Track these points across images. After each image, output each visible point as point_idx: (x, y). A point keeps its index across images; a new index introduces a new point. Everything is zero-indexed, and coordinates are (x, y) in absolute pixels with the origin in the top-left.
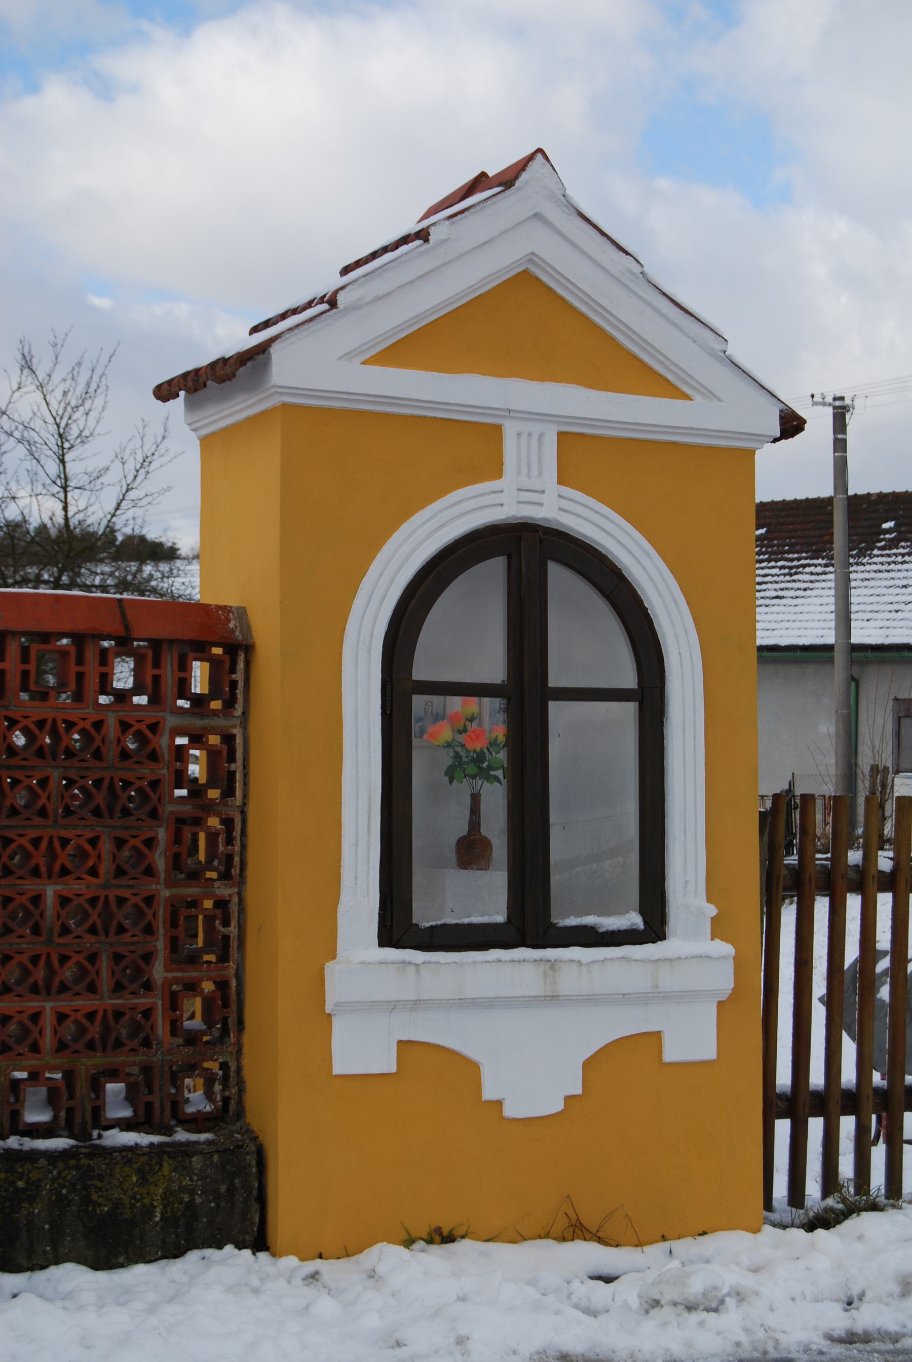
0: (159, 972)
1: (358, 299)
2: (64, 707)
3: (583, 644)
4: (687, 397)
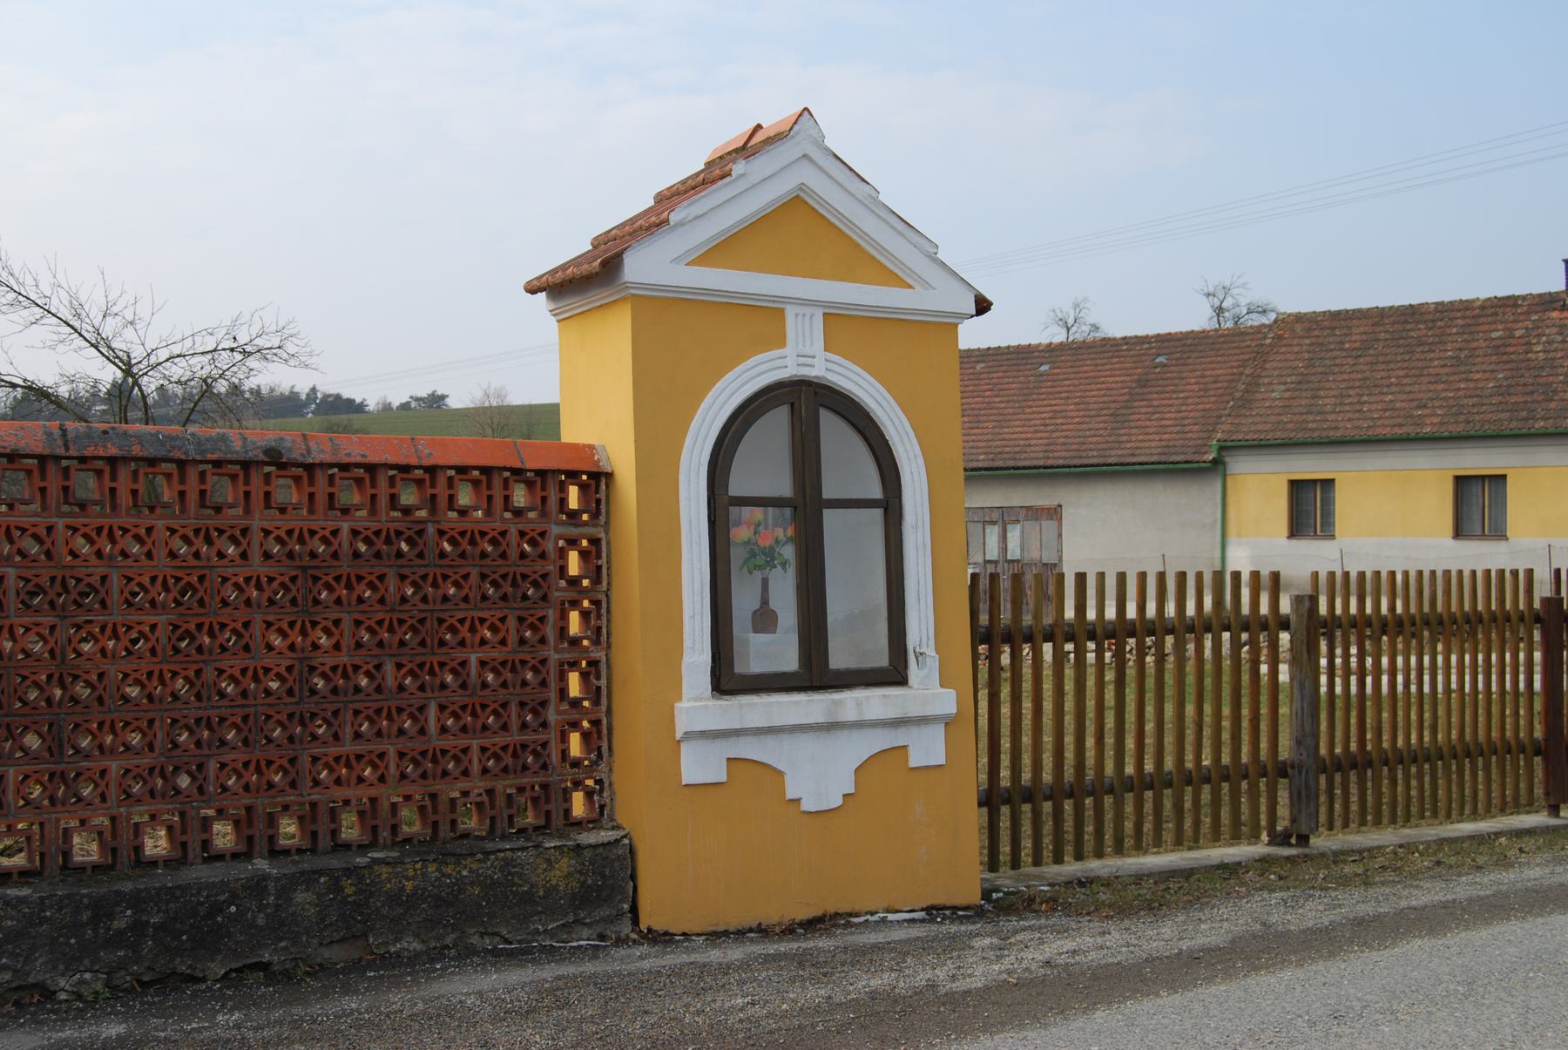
0: (552, 716)
2: (478, 521)
3: (845, 468)
4: (911, 287)
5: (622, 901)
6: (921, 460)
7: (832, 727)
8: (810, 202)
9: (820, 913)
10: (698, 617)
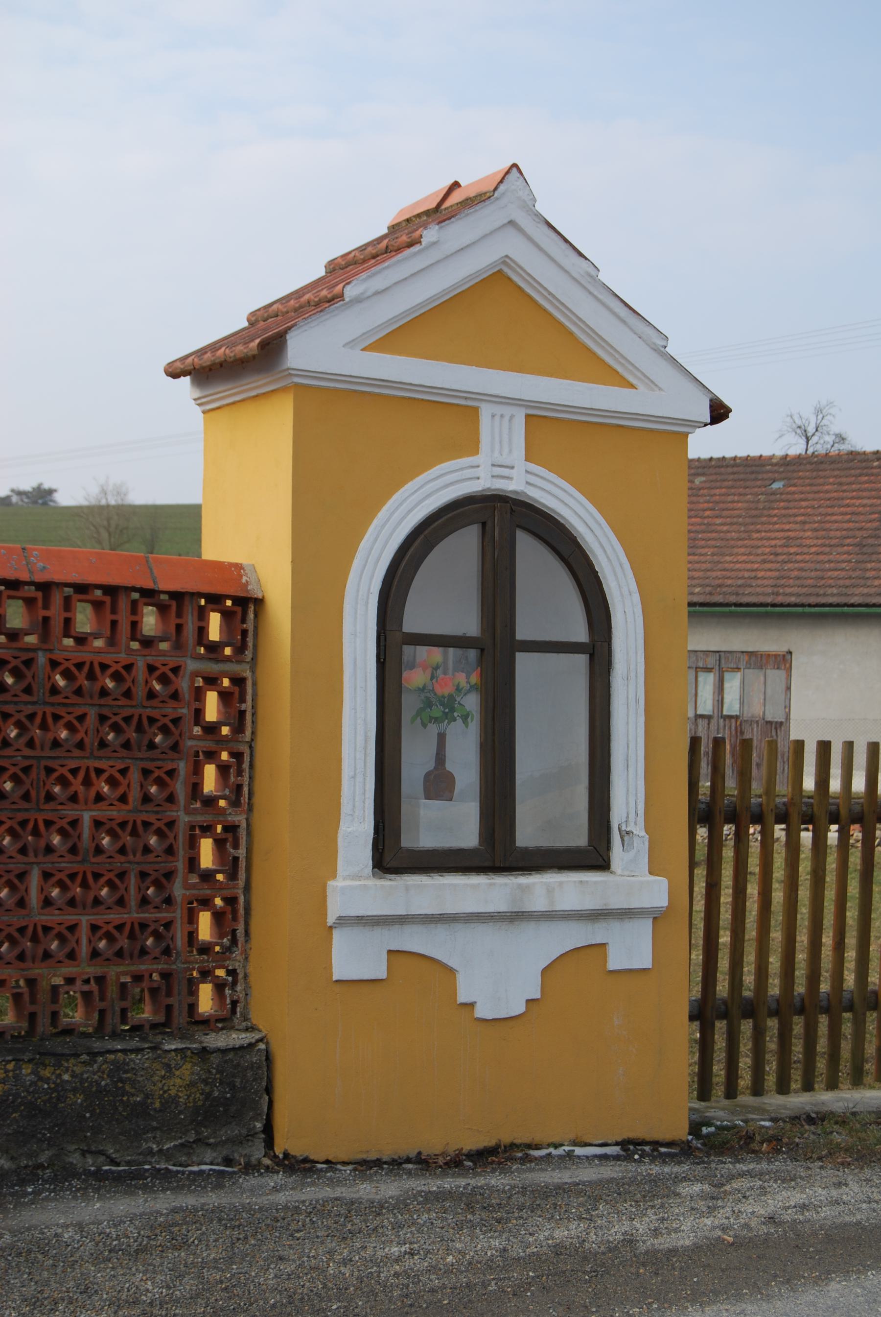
0: (178, 891)
1: (362, 294)
2: (99, 651)
3: (545, 604)
4: (632, 386)
5: (254, 1119)
6: (636, 597)
7: (515, 917)
8: (515, 278)
9: (492, 1143)
10: (359, 778)
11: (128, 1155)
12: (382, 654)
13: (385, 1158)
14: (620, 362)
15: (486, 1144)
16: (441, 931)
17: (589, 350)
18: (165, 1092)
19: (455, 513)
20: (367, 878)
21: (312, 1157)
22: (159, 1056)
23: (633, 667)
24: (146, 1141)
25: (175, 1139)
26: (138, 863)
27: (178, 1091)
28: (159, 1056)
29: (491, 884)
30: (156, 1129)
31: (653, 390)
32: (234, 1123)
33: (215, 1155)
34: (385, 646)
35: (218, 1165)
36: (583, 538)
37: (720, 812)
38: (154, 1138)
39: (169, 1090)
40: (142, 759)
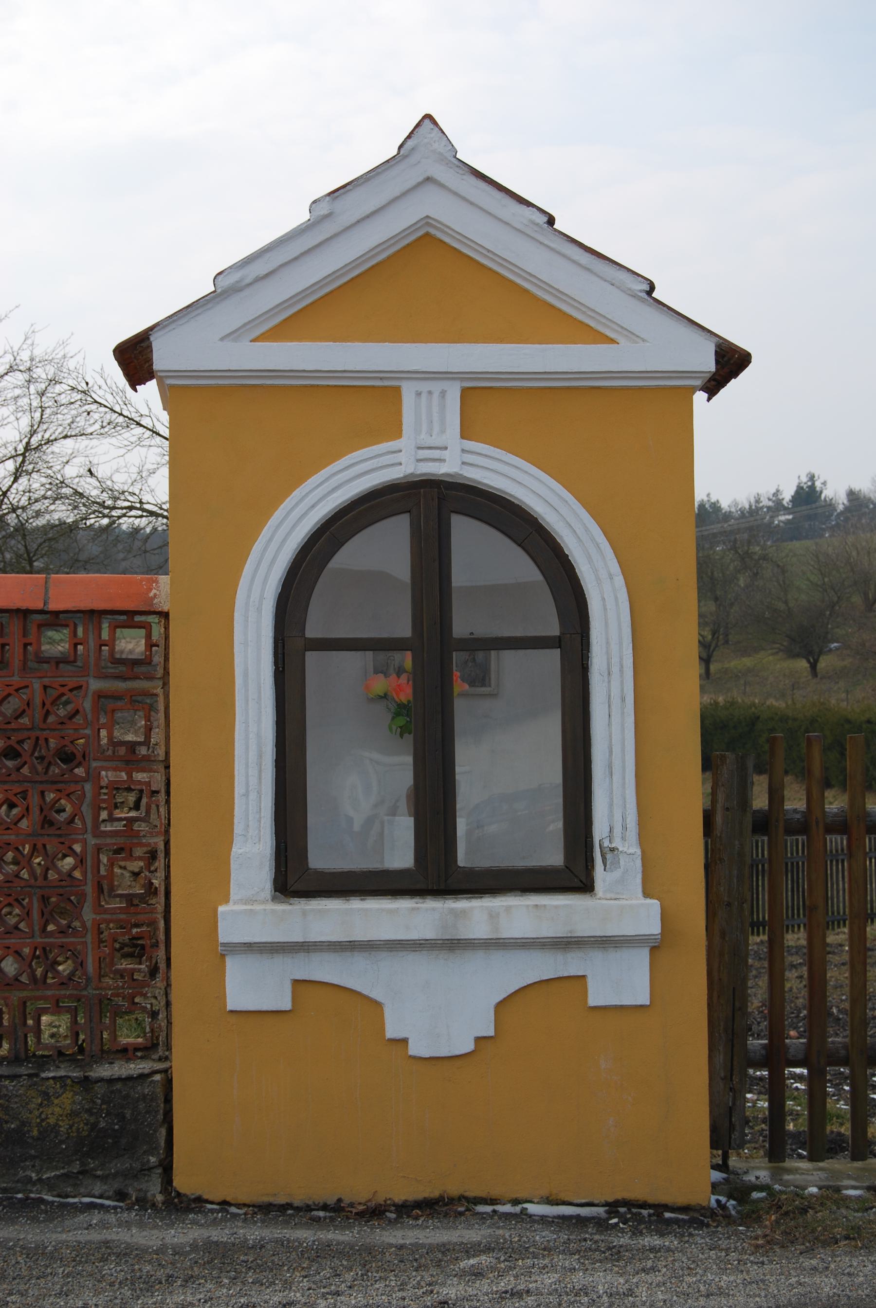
1: (237, 282)
4: (613, 341)
5: (150, 1152)
6: (620, 580)
7: (452, 945)
8: (447, 240)
9: (436, 1194)
10: (253, 796)
11: (4, 1182)
12: (280, 662)
13: (296, 1203)
14: (590, 316)
15: (426, 1195)
16: (360, 960)
17: (552, 307)
18: (42, 1120)
19: (373, 502)
20: (265, 902)
21: (205, 1197)
22: (35, 1084)
23: (615, 660)
24: (24, 1169)
25: (57, 1169)
26: (40, 887)
27: (58, 1120)
28: (35, 1084)
29: (413, 909)
30: (34, 1158)
31: (637, 343)
32: (126, 1156)
33: (106, 1187)
34: (284, 654)
35: (108, 1198)
36: (543, 519)
37: (817, 823)
38: (33, 1166)
39: (47, 1118)
40: (41, 782)
